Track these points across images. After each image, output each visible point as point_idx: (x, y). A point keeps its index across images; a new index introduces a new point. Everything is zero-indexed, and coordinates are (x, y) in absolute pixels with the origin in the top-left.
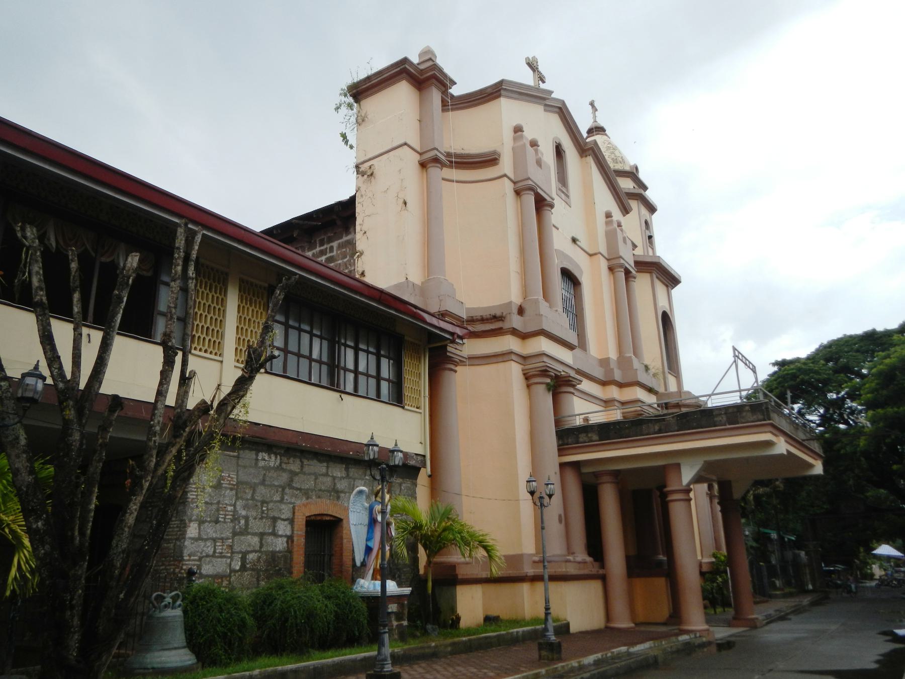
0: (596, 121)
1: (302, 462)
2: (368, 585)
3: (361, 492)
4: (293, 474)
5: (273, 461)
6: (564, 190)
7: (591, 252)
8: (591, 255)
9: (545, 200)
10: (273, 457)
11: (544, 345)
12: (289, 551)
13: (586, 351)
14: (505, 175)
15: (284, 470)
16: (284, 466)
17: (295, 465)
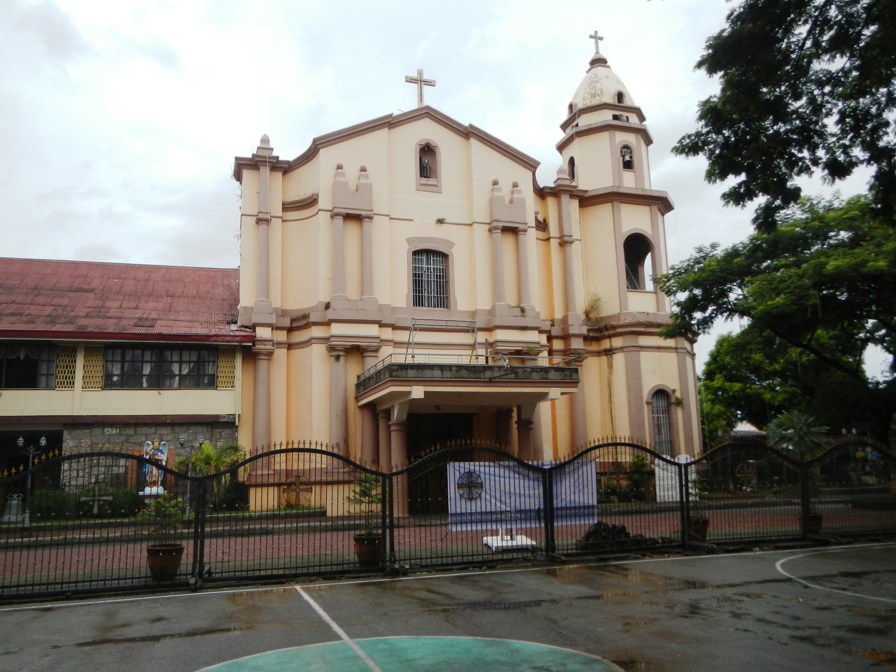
0: (597, 53)
1: (135, 430)
2: (148, 491)
3: (148, 444)
4: (129, 436)
5: (114, 431)
6: (431, 181)
7: (471, 223)
8: (471, 225)
9: (361, 215)
10: (114, 429)
11: (337, 329)
12: (126, 472)
13: (450, 309)
14: (319, 210)
15: (122, 435)
16: (122, 433)
17: (130, 431)
